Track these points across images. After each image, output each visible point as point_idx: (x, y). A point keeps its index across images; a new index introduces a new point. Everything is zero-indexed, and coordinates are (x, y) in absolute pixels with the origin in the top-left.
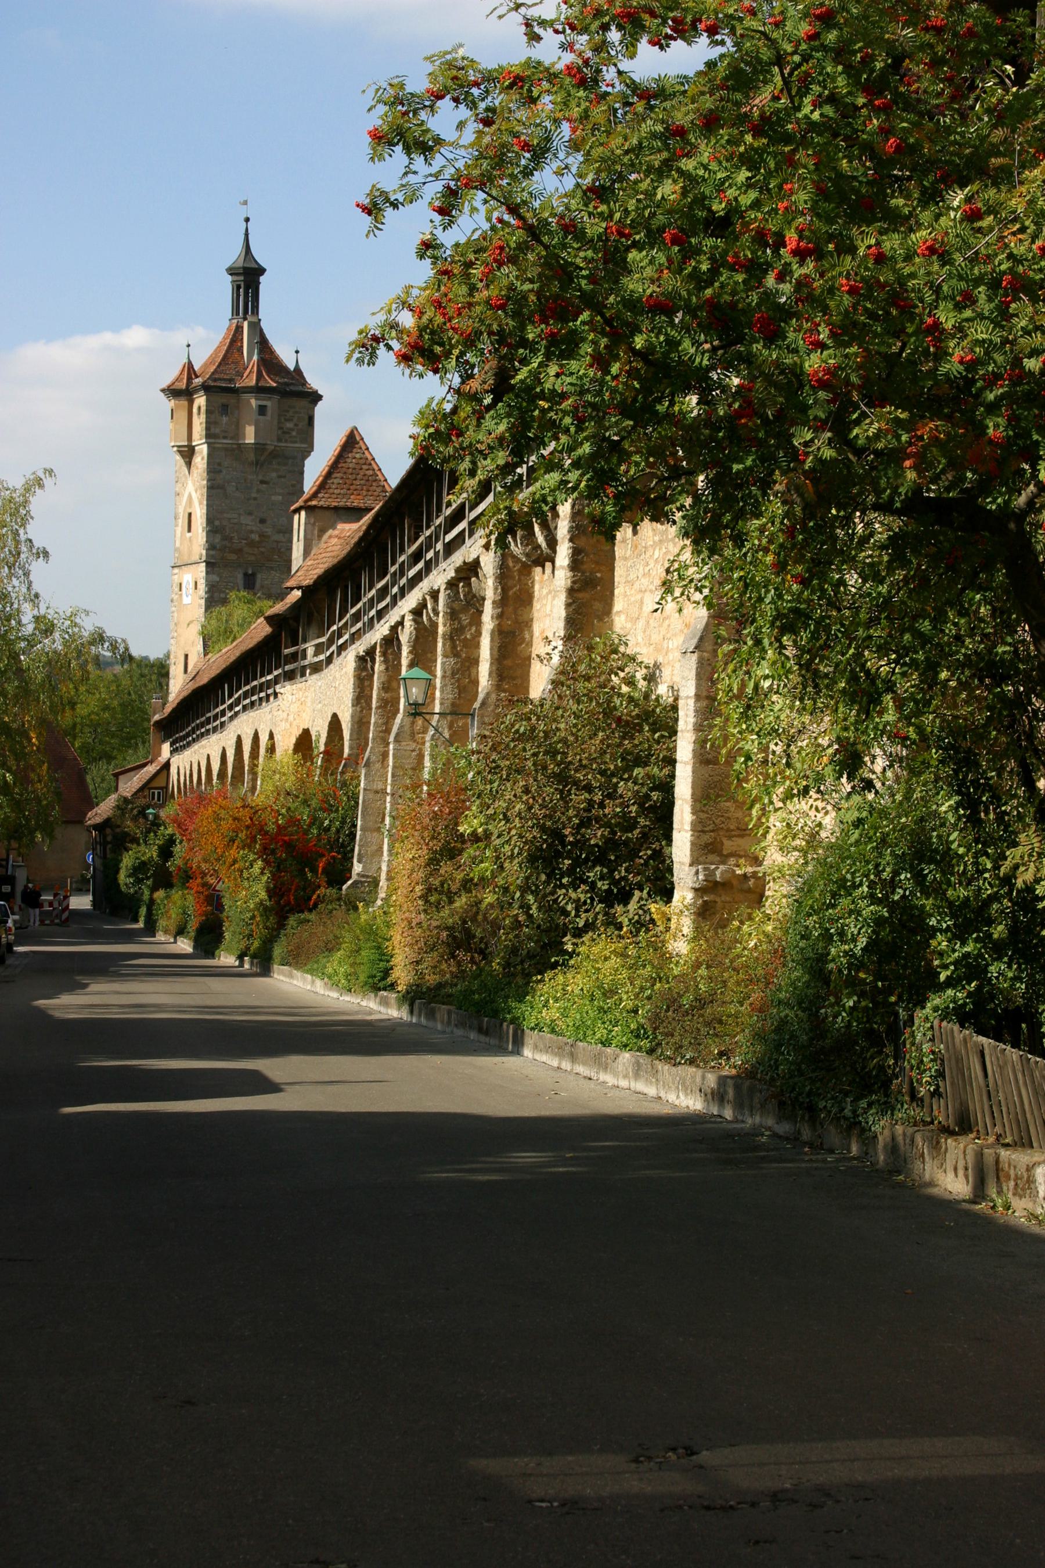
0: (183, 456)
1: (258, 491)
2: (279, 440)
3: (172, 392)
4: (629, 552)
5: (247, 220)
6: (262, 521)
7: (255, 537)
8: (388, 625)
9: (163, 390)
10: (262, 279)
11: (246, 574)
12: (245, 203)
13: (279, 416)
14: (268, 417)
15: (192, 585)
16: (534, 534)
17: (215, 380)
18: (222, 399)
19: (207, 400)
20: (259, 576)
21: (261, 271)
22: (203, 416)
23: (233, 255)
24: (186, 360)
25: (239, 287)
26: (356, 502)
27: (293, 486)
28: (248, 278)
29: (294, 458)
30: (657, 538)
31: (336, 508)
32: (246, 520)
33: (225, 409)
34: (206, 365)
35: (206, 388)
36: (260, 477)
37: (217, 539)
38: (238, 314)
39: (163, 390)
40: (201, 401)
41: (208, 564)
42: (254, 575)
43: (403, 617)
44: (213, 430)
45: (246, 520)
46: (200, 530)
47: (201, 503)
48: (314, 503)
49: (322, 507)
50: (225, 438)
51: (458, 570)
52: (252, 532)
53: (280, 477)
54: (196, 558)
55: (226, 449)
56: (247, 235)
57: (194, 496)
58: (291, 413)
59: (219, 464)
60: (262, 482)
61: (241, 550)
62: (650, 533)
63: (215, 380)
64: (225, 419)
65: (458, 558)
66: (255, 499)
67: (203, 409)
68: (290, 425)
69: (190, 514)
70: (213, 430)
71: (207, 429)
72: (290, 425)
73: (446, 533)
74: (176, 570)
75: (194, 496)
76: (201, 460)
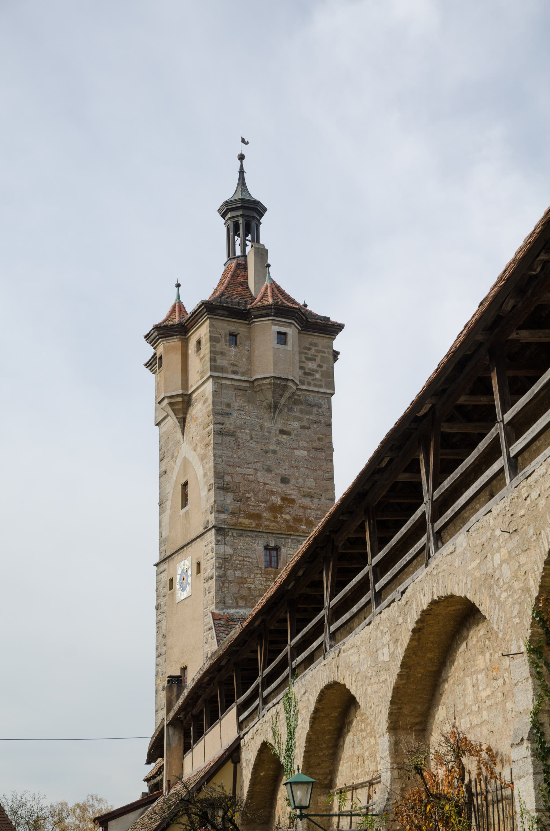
5: (241, 157)
7: (276, 500)
11: (267, 548)
14: (289, 347)
18: (228, 326)
19: (211, 326)
20: (283, 550)
27: (320, 439)
28: (244, 215)
32: (261, 476)
35: (209, 308)
36: (280, 426)
37: (229, 499)
40: (202, 332)
41: (219, 530)
42: (277, 549)
44: (219, 362)
45: (261, 476)
46: (204, 492)
50: (234, 372)
52: (272, 493)
55: (237, 389)
56: (242, 172)
58: (312, 352)
59: (228, 405)
60: (282, 432)
61: (257, 517)
66: (274, 452)
68: (311, 365)
70: (219, 362)
71: (213, 359)
72: (311, 365)
76: (201, 410)
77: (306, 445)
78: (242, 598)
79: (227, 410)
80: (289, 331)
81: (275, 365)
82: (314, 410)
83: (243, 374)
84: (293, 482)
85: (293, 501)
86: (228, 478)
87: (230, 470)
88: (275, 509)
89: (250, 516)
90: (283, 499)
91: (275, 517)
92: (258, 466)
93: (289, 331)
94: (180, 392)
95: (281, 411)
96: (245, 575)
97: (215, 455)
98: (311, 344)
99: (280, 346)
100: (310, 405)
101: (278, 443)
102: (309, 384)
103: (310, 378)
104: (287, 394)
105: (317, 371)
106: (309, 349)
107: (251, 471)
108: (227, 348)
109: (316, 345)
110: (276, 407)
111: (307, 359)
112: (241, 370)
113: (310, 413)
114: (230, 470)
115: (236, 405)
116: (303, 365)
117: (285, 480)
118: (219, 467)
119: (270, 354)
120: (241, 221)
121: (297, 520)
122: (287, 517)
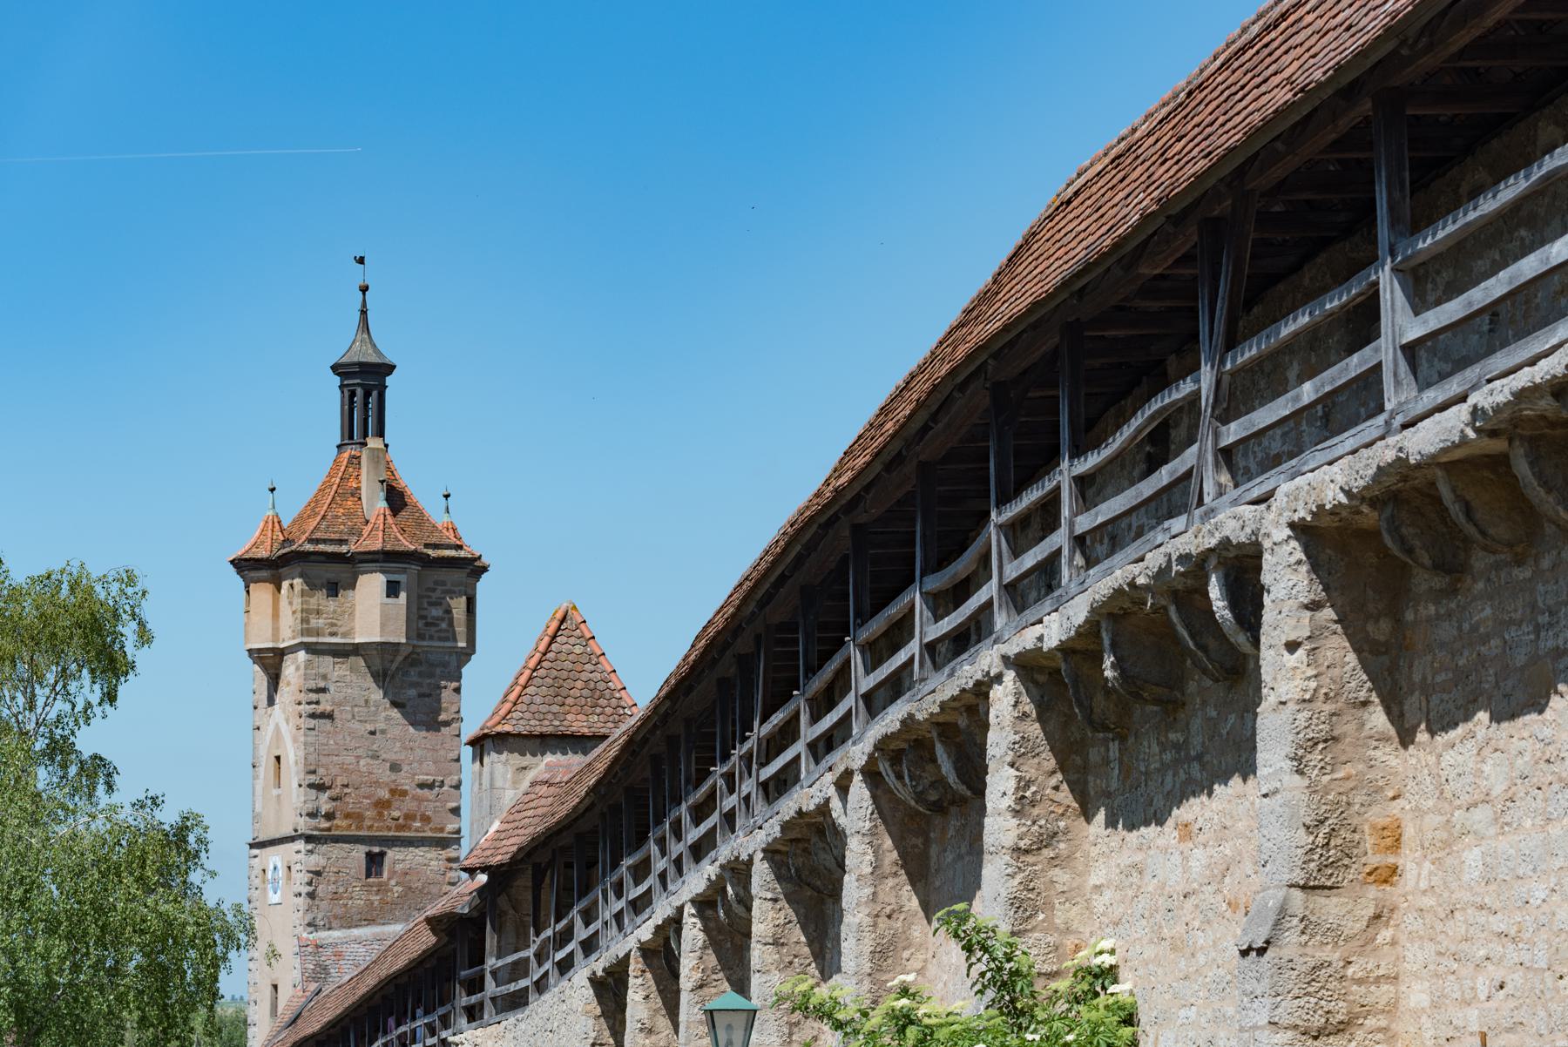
0: (265, 668)
1: (388, 719)
2: (421, 637)
3: (243, 565)
4: (1114, 785)
5: (364, 289)
6: (395, 767)
7: (384, 794)
8: (651, 924)
9: (232, 562)
10: (389, 380)
11: (369, 855)
12: (361, 261)
13: (420, 597)
15: (281, 873)
16: (934, 760)
17: (317, 541)
21: (390, 368)
22: (297, 601)
23: (341, 344)
24: (270, 513)
25: (353, 394)
26: (579, 724)
29: (445, 665)
30: (1168, 757)
31: (542, 736)
33: (333, 589)
34: (300, 519)
38: (351, 437)
39: (232, 562)
42: (382, 854)
43: (680, 910)
44: (315, 622)
46: (295, 785)
47: (295, 740)
48: (507, 728)
49: (519, 735)
50: (333, 634)
51: (785, 827)
53: (421, 695)
54: (287, 831)
56: (364, 312)
57: (287, 731)
58: (438, 594)
59: (324, 677)
62: (1156, 749)
63: (317, 541)
64: (331, 605)
65: (788, 806)
66: (383, 732)
67: (298, 588)
69: (278, 758)
71: (305, 621)
73: (762, 765)
74: (256, 852)
75: (284, 727)
77: (424, 718)
78: (335, 917)
79: (322, 684)
80: (402, 578)
81: (383, 625)
82: (438, 671)
83: (344, 635)
84: (405, 768)
85: (404, 793)
86: (321, 771)
87: (324, 760)
88: (382, 805)
89: (347, 816)
90: (393, 792)
91: (380, 814)
92: (360, 752)
93: (402, 578)
94: (270, 645)
95: (393, 677)
96: (341, 890)
97: (305, 744)
98: (436, 583)
99: (390, 600)
100: (432, 665)
101: (388, 719)
102: (431, 638)
103: (434, 629)
104: (400, 658)
105: (443, 619)
106: (434, 590)
107: (351, 759)
108: (323, 602)
109: (444, 583)
110: (385, 675)
111: (431, 604)
112: (341, 630)
113: (431, 675)
114: (324, 760)
115: (335, 675)
116: (423, 613)
117: (395, 767)
118: (312, 758)
119: (377, 611)
120: (359, 391)
121: (409, 817)
122: (396, 814)
